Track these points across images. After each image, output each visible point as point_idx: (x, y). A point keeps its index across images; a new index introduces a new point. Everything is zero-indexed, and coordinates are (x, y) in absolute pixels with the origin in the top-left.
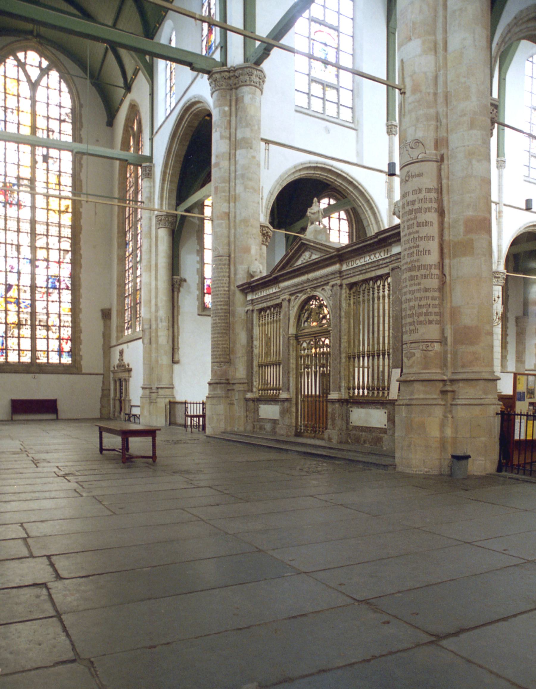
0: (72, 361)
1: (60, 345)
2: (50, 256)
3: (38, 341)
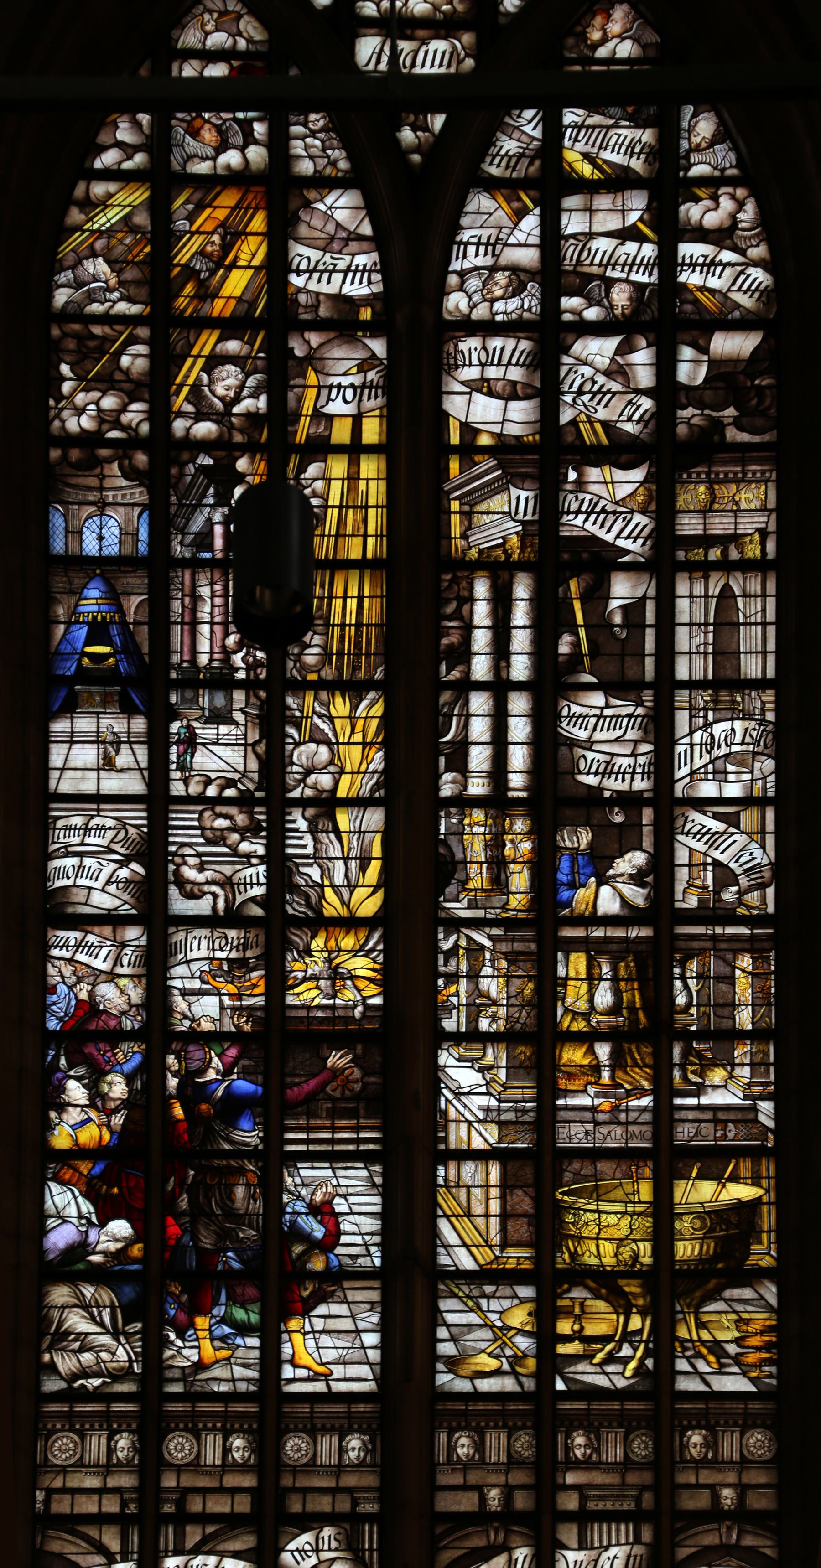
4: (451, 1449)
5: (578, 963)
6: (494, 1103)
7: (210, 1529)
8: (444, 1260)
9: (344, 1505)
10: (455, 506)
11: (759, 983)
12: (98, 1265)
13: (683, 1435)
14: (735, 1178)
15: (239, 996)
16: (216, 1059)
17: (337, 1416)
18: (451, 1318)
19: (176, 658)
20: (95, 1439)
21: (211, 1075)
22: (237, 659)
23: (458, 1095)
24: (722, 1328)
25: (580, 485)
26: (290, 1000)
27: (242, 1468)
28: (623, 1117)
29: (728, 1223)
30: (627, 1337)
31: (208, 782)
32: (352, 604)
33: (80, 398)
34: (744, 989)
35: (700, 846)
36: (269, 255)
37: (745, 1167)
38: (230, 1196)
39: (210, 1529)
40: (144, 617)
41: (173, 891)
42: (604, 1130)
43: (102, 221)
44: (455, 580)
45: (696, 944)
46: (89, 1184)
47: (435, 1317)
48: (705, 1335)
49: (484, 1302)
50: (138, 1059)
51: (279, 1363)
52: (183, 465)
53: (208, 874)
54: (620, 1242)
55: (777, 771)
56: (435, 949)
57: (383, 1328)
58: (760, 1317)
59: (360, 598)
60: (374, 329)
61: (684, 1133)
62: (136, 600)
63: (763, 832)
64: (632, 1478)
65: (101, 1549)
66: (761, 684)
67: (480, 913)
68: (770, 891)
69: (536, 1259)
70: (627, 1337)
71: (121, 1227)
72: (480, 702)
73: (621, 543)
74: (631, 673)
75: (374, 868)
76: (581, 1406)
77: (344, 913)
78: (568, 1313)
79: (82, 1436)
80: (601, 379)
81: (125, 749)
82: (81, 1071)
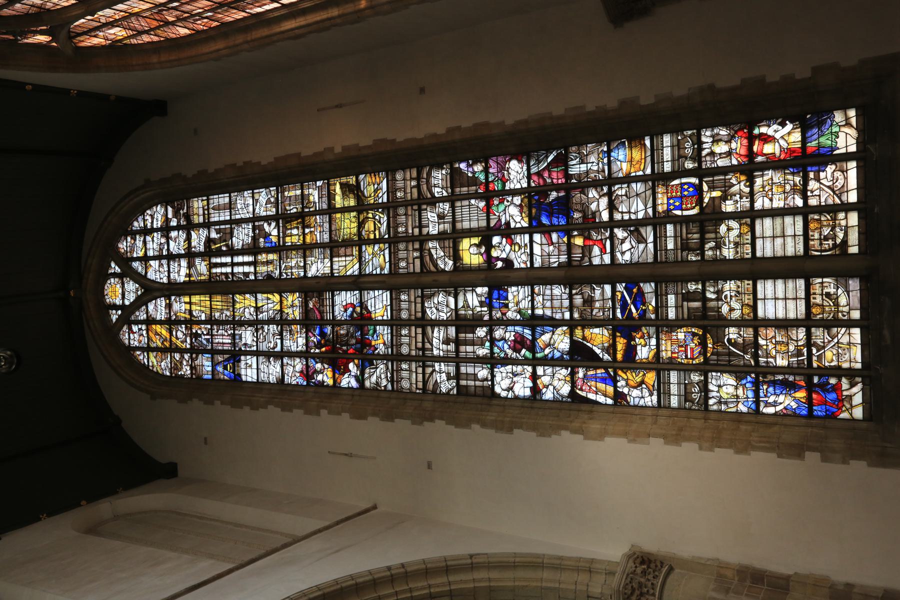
0: (844, 108)
1: (774, 163)
2: (474, 225)
3: (766, 249)
4: (404, 268)
5: (288, 239)
6: (320, 260)
7: (426, 341)
8: (356, 273)
9: (419, 300)
10: (199, 278)
11: (291, 189)
12: (360, 372)
13: (398, 199)
14: (335, 191)
15: (297, 332)
16: (312, 339)
17: (396, 303)
18: (371, 270)
19: (230, 348)
20: (403, 375)
21: (315, 340)
22: (229, 332)
23: (318, 271)
24: (371, 190)
25: (195, 247)
26: (298, 318)
27: (410, 330)
28: (322, 224)
29: (345, 191)
30: (374, 218)
31: (253, 340)
32: (218, 303)
33: (184, 370)
34: (292, 193)
35: (262, 209)
36: (159, 324)
37: (332, 188)
38: (343, 335)
39: (426, 341)
40: (222, 356)
41: (276, 350)
42: (325, 229)
43: (155, 363)
44: (213, 277)
45: (283, 207)
46: (341, 375)
47: (370, 275)
48: (373, 195)
49: (367, 260)
50: (312, 360)
51: (383, 320)
52: (195, 346)
53: (272, 340)
55: (247, 190)
56: (286, 279)
57: (374, 289)
58: (368, 179)
59: (217, 301)
60: (170, 299)
61: (325, 206)
62: (219, 358)
63: (259, 192)
64: (410, 213)
65: (432, 373)
66: (230, 197)
67: (278, 267)
68: (271, 189)
69: (356, 245)
70: (374, 218)
71: (351, 366)
72: (236, 269)
73: (205, 236)
74: (228, 231)
75: (270, 296)
76: (391, 229)
77: (279, 304)
78: (368, 235)
80: (177, 244)
81: (248, 362)
82: (315, 376)
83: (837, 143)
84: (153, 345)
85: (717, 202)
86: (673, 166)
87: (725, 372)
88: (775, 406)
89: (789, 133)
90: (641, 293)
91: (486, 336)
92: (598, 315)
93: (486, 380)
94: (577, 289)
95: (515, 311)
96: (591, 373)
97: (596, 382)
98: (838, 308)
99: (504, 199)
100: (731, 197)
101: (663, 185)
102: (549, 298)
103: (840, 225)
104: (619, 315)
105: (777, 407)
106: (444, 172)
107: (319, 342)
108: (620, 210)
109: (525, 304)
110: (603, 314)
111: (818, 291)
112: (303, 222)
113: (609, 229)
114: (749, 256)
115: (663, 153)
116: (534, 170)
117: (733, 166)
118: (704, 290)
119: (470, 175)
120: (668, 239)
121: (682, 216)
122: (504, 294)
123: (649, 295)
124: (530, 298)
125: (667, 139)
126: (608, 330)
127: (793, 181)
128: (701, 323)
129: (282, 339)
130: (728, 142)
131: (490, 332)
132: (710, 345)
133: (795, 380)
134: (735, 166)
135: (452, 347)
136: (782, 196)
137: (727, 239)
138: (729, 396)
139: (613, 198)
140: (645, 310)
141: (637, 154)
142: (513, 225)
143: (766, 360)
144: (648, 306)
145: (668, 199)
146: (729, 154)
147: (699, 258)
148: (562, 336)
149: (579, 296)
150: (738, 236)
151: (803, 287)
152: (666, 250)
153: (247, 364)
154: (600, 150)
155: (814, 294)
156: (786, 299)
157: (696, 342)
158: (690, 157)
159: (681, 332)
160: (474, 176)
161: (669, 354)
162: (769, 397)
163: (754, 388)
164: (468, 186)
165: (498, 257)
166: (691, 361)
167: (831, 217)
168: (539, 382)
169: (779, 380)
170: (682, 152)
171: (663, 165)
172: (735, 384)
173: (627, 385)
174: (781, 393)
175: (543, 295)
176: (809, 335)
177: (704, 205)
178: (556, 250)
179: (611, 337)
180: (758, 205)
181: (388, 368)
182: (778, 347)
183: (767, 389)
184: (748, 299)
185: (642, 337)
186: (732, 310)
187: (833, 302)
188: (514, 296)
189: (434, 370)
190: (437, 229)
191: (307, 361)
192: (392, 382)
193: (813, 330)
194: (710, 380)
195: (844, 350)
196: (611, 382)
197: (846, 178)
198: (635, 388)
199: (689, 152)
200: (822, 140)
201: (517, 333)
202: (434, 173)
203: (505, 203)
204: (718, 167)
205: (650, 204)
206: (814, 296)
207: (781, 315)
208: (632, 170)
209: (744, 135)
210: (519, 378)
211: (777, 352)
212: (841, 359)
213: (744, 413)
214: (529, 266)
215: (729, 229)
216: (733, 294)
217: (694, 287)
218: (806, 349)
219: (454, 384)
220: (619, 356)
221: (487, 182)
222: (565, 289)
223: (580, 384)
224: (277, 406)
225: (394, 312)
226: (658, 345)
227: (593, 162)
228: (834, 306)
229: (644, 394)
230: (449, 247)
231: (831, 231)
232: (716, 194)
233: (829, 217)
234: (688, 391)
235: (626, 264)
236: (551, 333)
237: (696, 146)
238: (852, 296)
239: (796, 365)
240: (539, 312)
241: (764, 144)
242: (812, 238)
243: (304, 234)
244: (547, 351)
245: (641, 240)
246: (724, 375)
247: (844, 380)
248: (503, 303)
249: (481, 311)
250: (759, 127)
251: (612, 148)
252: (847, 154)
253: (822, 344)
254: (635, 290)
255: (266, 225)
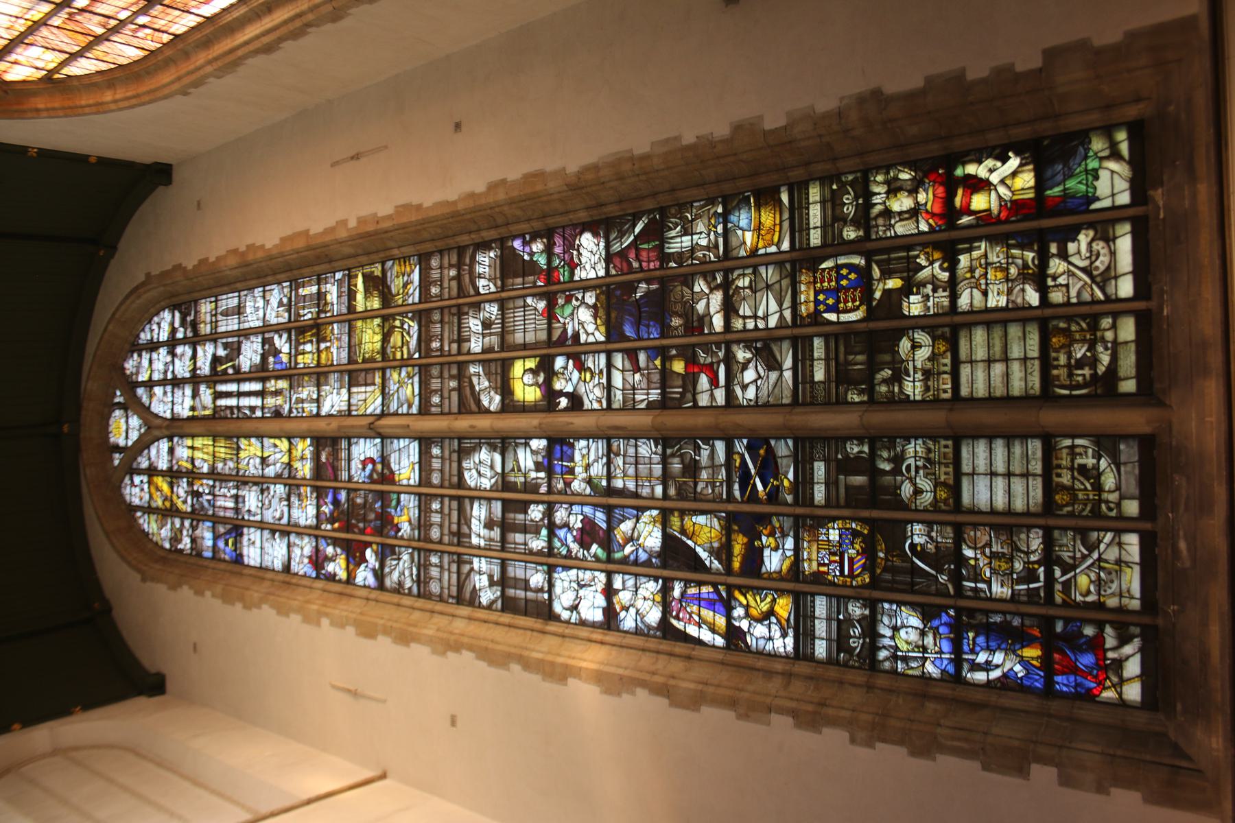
2: (530, 338)
3: (976, 381)
4: (437, 406)
7: (463, 521)
9: (455, 456)
23: (333, 406)
30: (402, 327)
37: (353, 282)
38: (360, 505)
48: (401, 291)
54: (374, 333)
56: (296, 417)
57: (398, 438)
64: (446, 319)
65: (469, 574)
71: (369, 553)
74: (236, 346)
75: (277, 442)
78: (394, 354)
79: (431, 578)
83: (1095, 188)
84: (154, 505)
85: (895, 296)
86: (824, 236)
87: (905, 604)
88: (987, 671)
89: (1014, 174)
90: (771, 458)
91: (542, 520)
92: (705, 492)
93: (541, 590)
94: (673, 447)
95: (584, 480)
96: (693, 591)
97: (700, 606)
98: (1100, 495)
99: (573, 295)
100: (918, 289)
101: (808, 269)
102: (633, 460)
103: (1103, 340)
104: (737, 494)
105: (990, 673)
106: (492, 254)
107: (332, 513)
108: (741, 313)
109: (598, 470)
110: (713, 491)
111: (1065, 462)
112: (317, 335)
113: (723, 346)
114: (948, 396)
115: (808, 214)
116: (616, 247)
117: (921, 233)
118: (873, 454)
119: (526, 257)
120: (815, 363)
121: (838, 323)
122: (569, 452)
123: (785, 461)
124: (605, 460)
125: (815, 190)
126: (719, 519)
127: (1022, 259)
128: (865, 514)
129: (289, 506)
130: (913, 192)
131: (549, 513)
132: (881, 555)
133: (1022, 623)
134: (924, 233)
135: (496, 533)
136: (1004, 287)
137: (911, 363)
138: (910, 648)
139: (731, 292)
140: (778, 487)
141: (767, 218)
142: (583, 338)
143: (973, 585)
144: (782, 481)
145: (817, 293)
146: (914, 213)
147: (865, 398)
148: (651, 526)
149: (677, 460)
150: (929, 359)
151: (1039, 454)
152: (812, 381)
153: (249, 539)
154: (712, 211)
155: (1059, 466)
156: (1009, 475)
157: (857, 546)
158: (851, 220)
159: (834, 528)
160: (531, 259)
161: (814, 565)
162: (978, 654)
163: (952, 636)
164: (523, 276)
165: (561, 390)
166: (848, 580)
167: (1088, 324)
168: (615, 600)
169: (995, 623)
170: (838, 212)
171: (808, 234)
172: (921, 626)
173: (747, 615)
174: (999, 648)
175: (624, 456)
176: (1048, 542)
177: (874, 303)
178: (645, 380)
179: (724, 532)
180: (964, 302)
181: (413, 561)
182: (995, 563)
183: (974, 639)
184: (945, 474)
185: (772, 534)
186: (918, 492)
187: (1092, 484)
188: (583, 456)
189: (472, 569)
190: (481, 344)
191: (317, 542)
192: (418, 581)
193: (1056, 534)
194: (879, 617)
195: (1110, 573)
196: (722, 609)
197: (1113, 254)
198: (760, 620)
199: (849, 210)
200: (1071, 184)
201: (585, 517)
202: (479, 258)
203: (574, 302)
204: (897, 236)
205: (787, 303)
206: (1059, 471)
207: (1000, 502)
208: (760, 245)
209: (939, 180)
210: (587, 592)
211: (994, 572)
212: (1105, 591)
213: (935, 679)
214: (605, 406)
215: (915, 346)
216: (920, 463)
217: (856, 449)
218: (1042, 569)
219: (499, 593)
220: (736, 565)
221: (551, 270)
222: (656, 447)
223: (675, 608)
224: (272, 606)
225: (423, 473)
226: (797, 549)
227: (701, 233)
228: (1093, 490)
229: (772, 634)
230: (496, 374)
231: (1088, 350)
232: (894, 283)
233: (1084, 325)
234: (843, 633)
235: (749, 406)
236: (634, 520)
237: (860, 201)
238: (1126, 472)
239: (1025, 599)
240: (619, 483)
241: (971, 194)
242: (1055, 363)
243: (319, 351)
244: (628, 549)
245: (773, 364)
246: (903, 608)
247: (1109, 630)
248: (567, 466)
249: (537, 478)
250: (964, 164)
251: (729, 207)
252: (1114, 208)
253: (1071, 561)
254: (762, 452)
255: (276, 337)
